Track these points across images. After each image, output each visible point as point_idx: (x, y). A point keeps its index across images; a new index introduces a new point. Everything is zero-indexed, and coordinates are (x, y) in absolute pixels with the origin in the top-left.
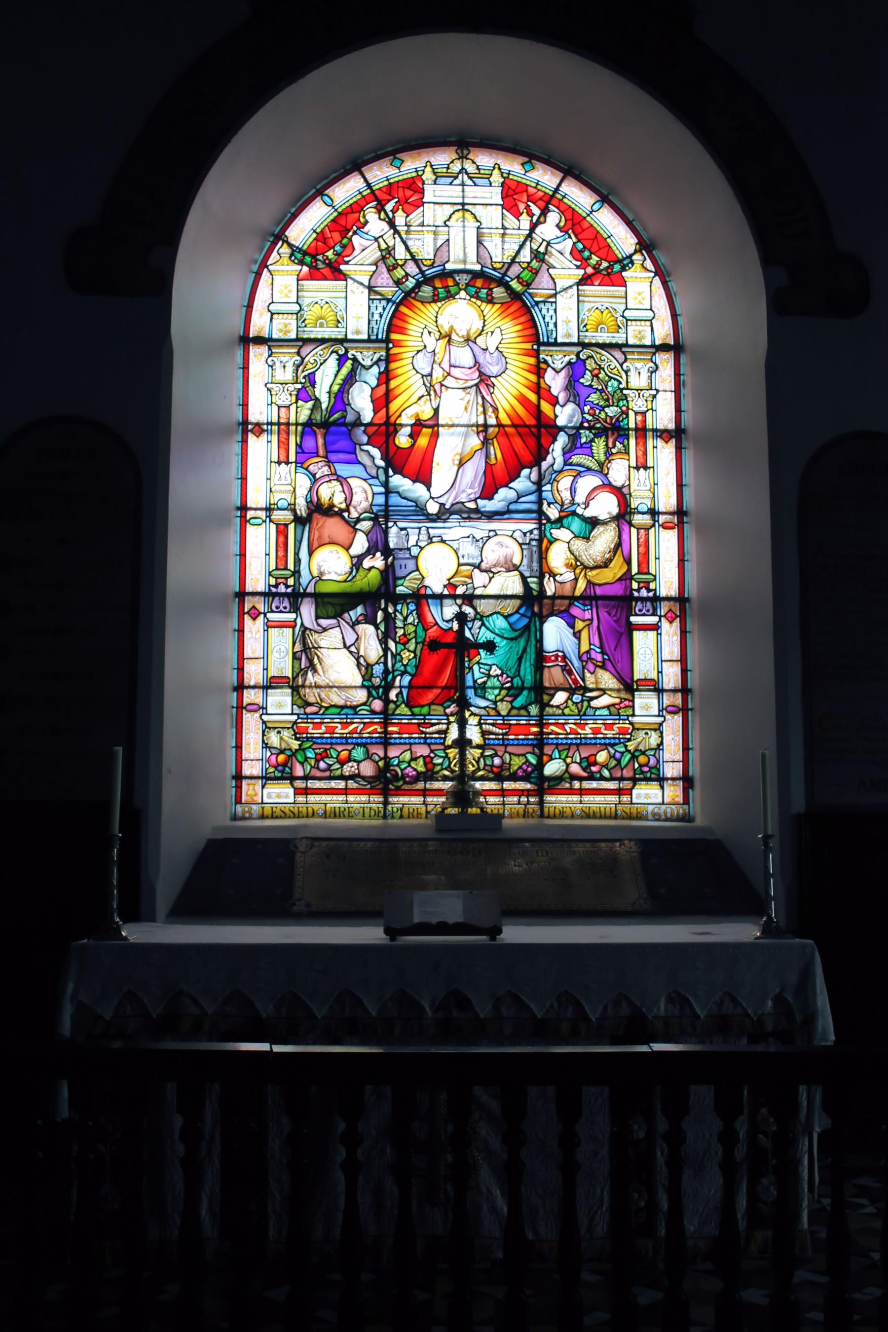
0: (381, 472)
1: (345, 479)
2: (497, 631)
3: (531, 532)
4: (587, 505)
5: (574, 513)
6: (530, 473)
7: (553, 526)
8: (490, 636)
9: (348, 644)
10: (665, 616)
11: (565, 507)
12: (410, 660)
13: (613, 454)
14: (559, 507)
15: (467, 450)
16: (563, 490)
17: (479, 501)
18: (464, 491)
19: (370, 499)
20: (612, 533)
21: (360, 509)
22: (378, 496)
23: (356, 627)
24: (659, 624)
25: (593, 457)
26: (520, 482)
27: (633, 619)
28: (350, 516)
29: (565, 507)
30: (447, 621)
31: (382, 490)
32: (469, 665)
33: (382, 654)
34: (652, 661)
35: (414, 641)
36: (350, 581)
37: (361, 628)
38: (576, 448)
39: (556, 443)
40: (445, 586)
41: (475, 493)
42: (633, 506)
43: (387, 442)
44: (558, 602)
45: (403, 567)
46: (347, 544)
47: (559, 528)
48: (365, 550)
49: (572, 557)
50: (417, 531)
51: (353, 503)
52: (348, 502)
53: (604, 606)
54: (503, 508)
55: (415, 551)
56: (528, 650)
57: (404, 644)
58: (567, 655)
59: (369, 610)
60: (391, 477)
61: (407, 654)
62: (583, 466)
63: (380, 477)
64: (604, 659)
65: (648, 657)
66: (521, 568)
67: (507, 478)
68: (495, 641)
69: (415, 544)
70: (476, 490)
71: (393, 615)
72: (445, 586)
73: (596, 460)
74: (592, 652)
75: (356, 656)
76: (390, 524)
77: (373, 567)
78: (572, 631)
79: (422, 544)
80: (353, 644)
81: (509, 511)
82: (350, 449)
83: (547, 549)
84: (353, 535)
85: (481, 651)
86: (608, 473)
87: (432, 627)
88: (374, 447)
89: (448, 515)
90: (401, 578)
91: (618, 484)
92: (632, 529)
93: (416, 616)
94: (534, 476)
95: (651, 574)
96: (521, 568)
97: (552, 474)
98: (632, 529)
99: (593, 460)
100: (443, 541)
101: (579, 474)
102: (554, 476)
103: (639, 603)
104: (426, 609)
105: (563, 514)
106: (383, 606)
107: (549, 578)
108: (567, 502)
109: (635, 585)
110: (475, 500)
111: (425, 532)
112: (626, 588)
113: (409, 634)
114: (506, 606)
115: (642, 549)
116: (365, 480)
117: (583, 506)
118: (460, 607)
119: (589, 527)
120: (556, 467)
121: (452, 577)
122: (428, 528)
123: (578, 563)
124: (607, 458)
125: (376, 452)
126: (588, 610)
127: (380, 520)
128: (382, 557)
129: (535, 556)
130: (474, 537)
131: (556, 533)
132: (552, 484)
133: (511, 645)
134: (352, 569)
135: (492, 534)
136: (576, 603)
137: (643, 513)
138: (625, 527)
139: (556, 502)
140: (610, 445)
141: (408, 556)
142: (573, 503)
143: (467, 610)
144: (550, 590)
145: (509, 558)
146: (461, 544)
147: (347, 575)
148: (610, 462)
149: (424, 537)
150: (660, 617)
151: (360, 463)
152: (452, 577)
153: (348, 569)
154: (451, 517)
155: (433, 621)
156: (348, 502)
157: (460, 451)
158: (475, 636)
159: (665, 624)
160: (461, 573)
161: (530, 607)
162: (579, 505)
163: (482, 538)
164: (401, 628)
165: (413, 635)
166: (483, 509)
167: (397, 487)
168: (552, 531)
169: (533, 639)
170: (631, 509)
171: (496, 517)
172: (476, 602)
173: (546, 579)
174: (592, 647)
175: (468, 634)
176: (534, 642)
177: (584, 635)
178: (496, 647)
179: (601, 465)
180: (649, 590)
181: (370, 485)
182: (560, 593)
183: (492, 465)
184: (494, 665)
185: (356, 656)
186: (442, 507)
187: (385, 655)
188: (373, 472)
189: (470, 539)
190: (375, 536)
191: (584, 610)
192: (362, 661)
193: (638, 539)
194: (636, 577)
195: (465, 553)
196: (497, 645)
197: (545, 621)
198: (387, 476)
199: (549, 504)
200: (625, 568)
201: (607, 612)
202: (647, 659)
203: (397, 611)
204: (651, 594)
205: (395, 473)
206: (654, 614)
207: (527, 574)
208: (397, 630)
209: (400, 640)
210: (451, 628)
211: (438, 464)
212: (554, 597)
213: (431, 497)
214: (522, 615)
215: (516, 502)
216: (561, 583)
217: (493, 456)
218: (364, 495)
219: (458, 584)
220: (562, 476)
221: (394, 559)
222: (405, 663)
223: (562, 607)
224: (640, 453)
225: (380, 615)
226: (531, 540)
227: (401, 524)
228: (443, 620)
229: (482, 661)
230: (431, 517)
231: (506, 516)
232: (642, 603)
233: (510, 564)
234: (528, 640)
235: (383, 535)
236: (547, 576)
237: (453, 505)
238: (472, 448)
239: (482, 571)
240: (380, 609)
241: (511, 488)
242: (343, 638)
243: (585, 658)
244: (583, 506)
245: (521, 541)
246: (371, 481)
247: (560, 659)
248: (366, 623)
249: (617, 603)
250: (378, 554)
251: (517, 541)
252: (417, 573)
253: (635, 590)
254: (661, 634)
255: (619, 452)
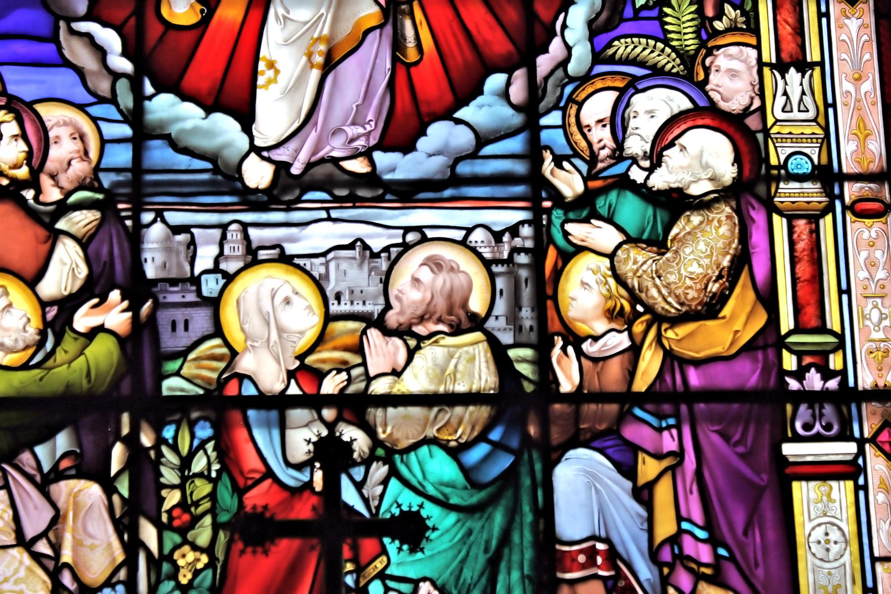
0: (123, 86)
1: (30, 105)
2: (431, 490)
3: (514, 230)
4: (655, 159)
5: (624, 183)
6: (508, 84)
7: (571, 215)
8: (410, 500)
9: (30, 533)
10: (873, 440)
11: (600, 165)
12: (197, 573)
13: (717, 33)
14: (584, 168)
15: (346, 28)
16: (592, 123)
17: (378, 156)
18: (338, 131)
19: (94, 154)
20: (724, 230)
21: (66, 181)
22: (116, 146)
23: (54, 489)
24: (860, 461)
25: (666, 42)
26: (481, 107)
27: (789, 449)
28: (42, 198)
29: (600, 165)
30: (299, 467)
31: (126, 131)
32: (357, 582)
33: (120, 557)
34: (846, 558)
35: (208, 520)
36: (38, 366)
37: (63, 489)
38: (623, 20)
39: (572, 10)
40: (291, 374)
41: (368, 135)
42: (774, 161)
43: (139, 13)
44: (590, 408)
45: (180, 326)
46: (29, 268)
47: (586, 221)
48: (78, 284)
49: (623, 292)
50: (217, 233)
51: (50, 165)
52: (36, 162)
53: (712, 419)
54: (443, 172)
55: (211, 286)
56: (516, 538)
57: (183, 531)
58: (620, 549)
59: (89, 440)
60: (150, 98)
61: (191, 556)
62: (642, 64)
63: (120, 100)
64: (717, 557)
65: (835, 549)
66: (491, 324)
67: (449, 98)
68: (424, 513)
69: (210, 265)
70: (368, 128)
71: (152, 454)
72: (291, 374)
73: (673, 49)
74: (687, 539)
75: (51, 565)
76: (147, 217)
77: (100, 329)
78: (629, 484)
79: (230, 267)
80: (44, 535)
81: (456, 180)
82: (44, 29)
83: (558, 273)
84: (48, 245)
85: (386, 540)
86: (706, 81)
87: (258, 482)
88: (105, 24)
89: (297, 192)
90: (174, 356)
91: (735, 105)
92: (776, 218)
93: (213, 455)
94: (518, 92)
95: (832, 333)
96: (491, 324)
97: (563, 87)
98: (776, 218)
99: (668, 50)
100: (285, 259)
101: (632, 86)
102: (568, 90)
103: (803, 408)
104: (242, 434)
105: (595, 184)
106: (125, 430)
107: (564, 349)
108: (604, 153)
109: (790, 362)
110: (367, 154)
111: (240, 236)
112: (765, 371)
113: (197, 504)
114: (454, 421)
115: (803, 269)
116: (81, 107)
117: (646, 164)
118: (331, 426)
119: (662, 216)
120: (576, 67)
121: (311, 350)
122: (245, 226)
123: (640, 308)
124: (702, 44)
125: (110, 38)
126: (669, 427)
127: (121, 206)
128: (126, 304)
129: (527, 293)
130: (366, 247)
131: (577, 231)
132: (564, 110)
133: (469, 524)
134: (43, 334)
135: (411, 237)
136: (638, 412)
137: (800, 178)
138: (758, 216)
139: (576, 155)
140: (710, 12)
141: (191, 297)
142: (618, 154)
143: (349, 433)
144: (569, 378)
145: (457, 299)
146: (332, 265)
147: (30, 352)
148: (709, 53)
149: (234, 246)
150: (861, 442)
151: (66, 63)
152: (311, 350)
153: (32, 334)
154: (305, 197)
155: (260, 466)
156: (36, 162)
157: (326, 31)
158: (374, 504)
159: (875, 462)
160: (332, 338)
161: (518, 424)
162: (634, 160)
163: (386, 249)
164: (173, 487)
165: (206, 505)
166: (388, 177)
167: (163, 124)
168: (569, 227)
169: (526, 508)
170: (770, 167)
171: (422, 196)
172: (376, 414)
173: (556, 352)
174: (685, 525)
175: (349, 495)
176: (529, 518)
177: (663, 493)
178: (427, 528)
179: (687, 59)
180: (827, 374)
181: (95, 120)
182: (594, 384)
183: (409, 66)
184: (424, 579)
185: (51, 565)
186: (283, 172)
187: (130, 563)
188: (104, 86)
189: (356, 253)
190: (105, 250)
191: (660, 430)
192: (67, 579)
193: (792, 244)
194: (792, 339)
195: (342, 287)
196: (429, 523)
197: (558, 461)
198: (140, 98)
199: (558, 161)
200: (761, 319)
201: (721, 433)
202: (831, 556)
203: (165, 441)
204: (833, 384)
205: (160, 89)
206: (845, 436)
207: (506, 338)
208: (164, 493)
209: (171, 518)
210: (309, 485)
211: (271, 65)
212: (578, 397)
213: (254, 149)
214: (497, 446)
215: (474, 155)
216: (595, 360)
217: (411, 43)
218: (77, 145)
219: (326, 367)
220: (590, 90)
221: (157, 306)
222: (184, 581)
223: (600, 423)
224: (786, 30)
225: (118, 454)
226: (515, 250)
227: (175, 218)
228: (288, 464)
229: (392, 571)
230: (252, 198)
231: (448, 193)
232: (811, 407)
233: (462, 313)
234: (513, 513)
235: (126, 245)
236: (559, 342)
237: (309, 166)
238: (357, 25)
239: (387, 332)
240: (118, 437)
241: (459, 122)
242: (16, 518)
243: (666, 555)
244: (646, 164)
245: (488, 255)
246: (96, 111)
247: (599, 560)
248: (78, 476)
249: (747, 407)
250: (115, 295)
251: (479, 255)
252: (217, 341)
253: (791, 374)
254: (865, 488)
255: (733, 29)
